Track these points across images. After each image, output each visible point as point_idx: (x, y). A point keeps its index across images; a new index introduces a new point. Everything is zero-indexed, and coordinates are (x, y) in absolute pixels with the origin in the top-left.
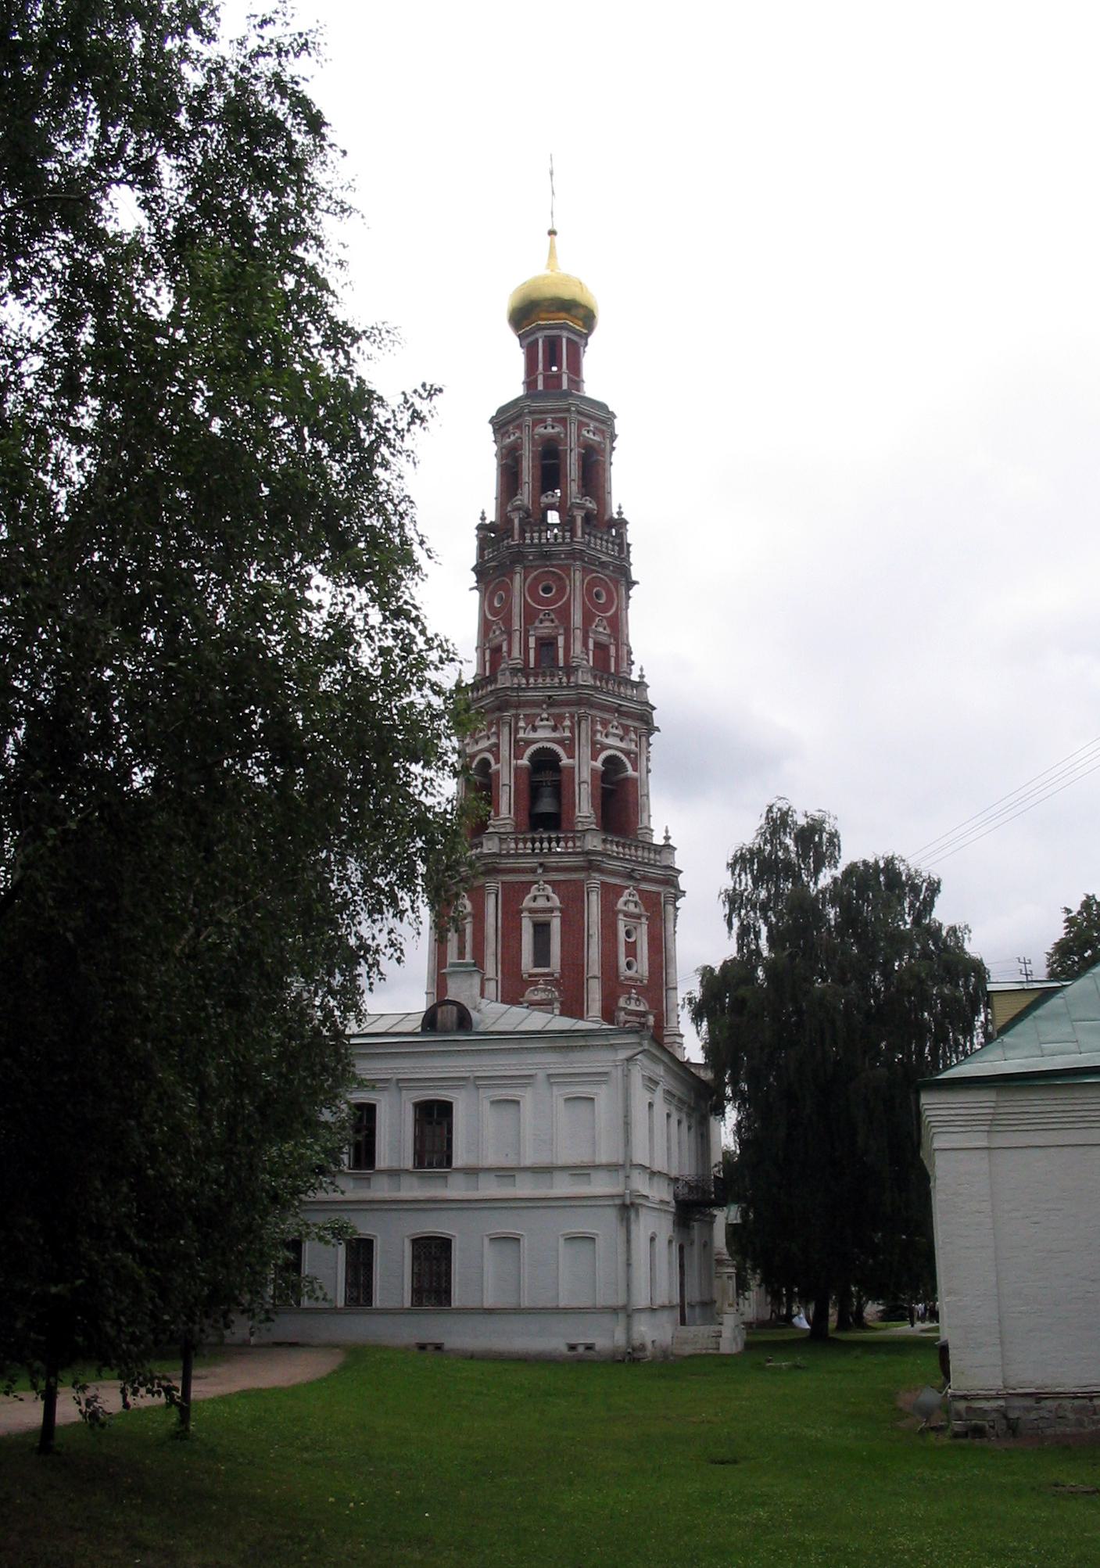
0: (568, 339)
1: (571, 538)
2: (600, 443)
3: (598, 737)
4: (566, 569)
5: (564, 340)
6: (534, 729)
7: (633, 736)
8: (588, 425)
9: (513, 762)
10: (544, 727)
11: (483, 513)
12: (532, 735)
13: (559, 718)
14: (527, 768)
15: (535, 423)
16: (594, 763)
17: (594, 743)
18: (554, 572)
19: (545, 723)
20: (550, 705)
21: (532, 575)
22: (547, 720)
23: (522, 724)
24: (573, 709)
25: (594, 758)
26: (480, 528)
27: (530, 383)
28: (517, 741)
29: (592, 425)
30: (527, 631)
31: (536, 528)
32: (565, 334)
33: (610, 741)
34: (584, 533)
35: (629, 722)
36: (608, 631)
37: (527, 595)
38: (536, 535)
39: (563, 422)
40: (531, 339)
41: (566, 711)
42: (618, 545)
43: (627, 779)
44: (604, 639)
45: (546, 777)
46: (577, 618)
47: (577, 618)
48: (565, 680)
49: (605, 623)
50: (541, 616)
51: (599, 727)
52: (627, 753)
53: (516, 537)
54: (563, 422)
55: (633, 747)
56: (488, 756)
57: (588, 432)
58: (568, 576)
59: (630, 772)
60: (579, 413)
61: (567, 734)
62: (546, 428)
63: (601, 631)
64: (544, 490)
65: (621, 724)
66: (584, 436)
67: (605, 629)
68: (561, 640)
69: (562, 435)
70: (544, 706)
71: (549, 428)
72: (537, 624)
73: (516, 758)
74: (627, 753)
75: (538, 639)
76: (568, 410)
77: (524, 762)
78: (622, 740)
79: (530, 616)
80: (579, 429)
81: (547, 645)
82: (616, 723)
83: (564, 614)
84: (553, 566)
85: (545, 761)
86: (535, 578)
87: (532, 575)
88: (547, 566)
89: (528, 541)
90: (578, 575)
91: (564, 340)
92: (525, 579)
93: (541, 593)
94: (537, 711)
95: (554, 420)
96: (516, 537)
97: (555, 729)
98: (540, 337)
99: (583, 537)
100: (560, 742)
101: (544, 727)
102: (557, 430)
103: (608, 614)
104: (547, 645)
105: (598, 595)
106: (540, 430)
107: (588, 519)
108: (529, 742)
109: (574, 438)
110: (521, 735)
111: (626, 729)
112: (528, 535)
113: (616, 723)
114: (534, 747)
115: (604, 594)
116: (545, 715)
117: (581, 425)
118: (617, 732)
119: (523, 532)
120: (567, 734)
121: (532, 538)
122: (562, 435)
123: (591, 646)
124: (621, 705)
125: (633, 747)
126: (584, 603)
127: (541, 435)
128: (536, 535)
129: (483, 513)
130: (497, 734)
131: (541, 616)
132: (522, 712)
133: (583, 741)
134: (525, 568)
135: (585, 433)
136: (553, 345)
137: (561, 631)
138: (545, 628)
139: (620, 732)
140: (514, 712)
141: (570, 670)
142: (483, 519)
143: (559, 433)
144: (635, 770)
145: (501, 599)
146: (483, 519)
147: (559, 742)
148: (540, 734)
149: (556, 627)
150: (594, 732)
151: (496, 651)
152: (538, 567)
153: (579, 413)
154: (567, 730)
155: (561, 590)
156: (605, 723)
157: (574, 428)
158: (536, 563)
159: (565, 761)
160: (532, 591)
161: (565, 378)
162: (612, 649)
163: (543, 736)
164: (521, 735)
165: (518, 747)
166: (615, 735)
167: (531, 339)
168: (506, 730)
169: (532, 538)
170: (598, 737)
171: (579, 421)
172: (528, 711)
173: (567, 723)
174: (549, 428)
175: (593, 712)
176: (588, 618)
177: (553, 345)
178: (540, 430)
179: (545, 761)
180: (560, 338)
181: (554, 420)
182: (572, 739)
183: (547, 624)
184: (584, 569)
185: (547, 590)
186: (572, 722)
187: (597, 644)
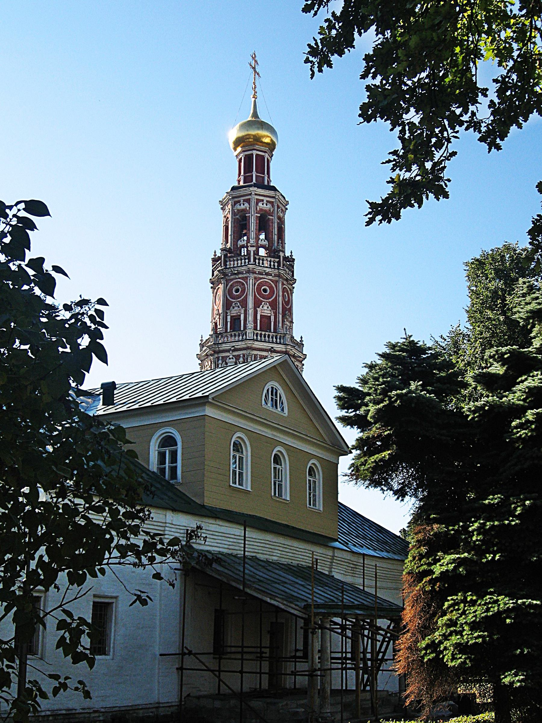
0: (257, 155)
1: (249, 262)
4: (245, 279)
10: (231, 362)
11: (215, 252)
15: (235, 203)
18: (240, 282)
19: (231, 360)
20: (233, 351)
21: (230, 284)
22: (233, 358)
29: (265, 199)
30: (227, 313)
31: (232, 259)
32: (255, 153)
39: (248, 201)
54: (248, 201)
57: (263, 204)
58: (247, 283)
60: (256, 194)
62: (240, 205)
63: (265, 310)
69: (248, 208)
75: (231, 317)
76: (250, 194)
84: (239, 278)
87: (230, 284)
88: (237, 279)
92: (227, 286)
93: (234, 293)
94: (228, 354)
95: (244, 201)
99: (255, 261)
105: (265, 290)
106: (238, 207)
112: (228, 263)
115: (268, 288)
116: (231, 357)
117: (258, 201)
121: (230, 264)
122: (248, 208)
124: (272, 348)
127: (238, 210)
128: (232, 263)
129: (215, 252)
136: (248, 159)
138: (234, 312)
142: (215, 255)
146: (215, 255)
153: (256, 194)
155: (243, 291)
158: (232, 277)
174: (242, 205)
175: (255, 352)
176: (257, 304)
178: (238, 207)
180: (252, 154)
184: (255, 278)
185: (237, 291)
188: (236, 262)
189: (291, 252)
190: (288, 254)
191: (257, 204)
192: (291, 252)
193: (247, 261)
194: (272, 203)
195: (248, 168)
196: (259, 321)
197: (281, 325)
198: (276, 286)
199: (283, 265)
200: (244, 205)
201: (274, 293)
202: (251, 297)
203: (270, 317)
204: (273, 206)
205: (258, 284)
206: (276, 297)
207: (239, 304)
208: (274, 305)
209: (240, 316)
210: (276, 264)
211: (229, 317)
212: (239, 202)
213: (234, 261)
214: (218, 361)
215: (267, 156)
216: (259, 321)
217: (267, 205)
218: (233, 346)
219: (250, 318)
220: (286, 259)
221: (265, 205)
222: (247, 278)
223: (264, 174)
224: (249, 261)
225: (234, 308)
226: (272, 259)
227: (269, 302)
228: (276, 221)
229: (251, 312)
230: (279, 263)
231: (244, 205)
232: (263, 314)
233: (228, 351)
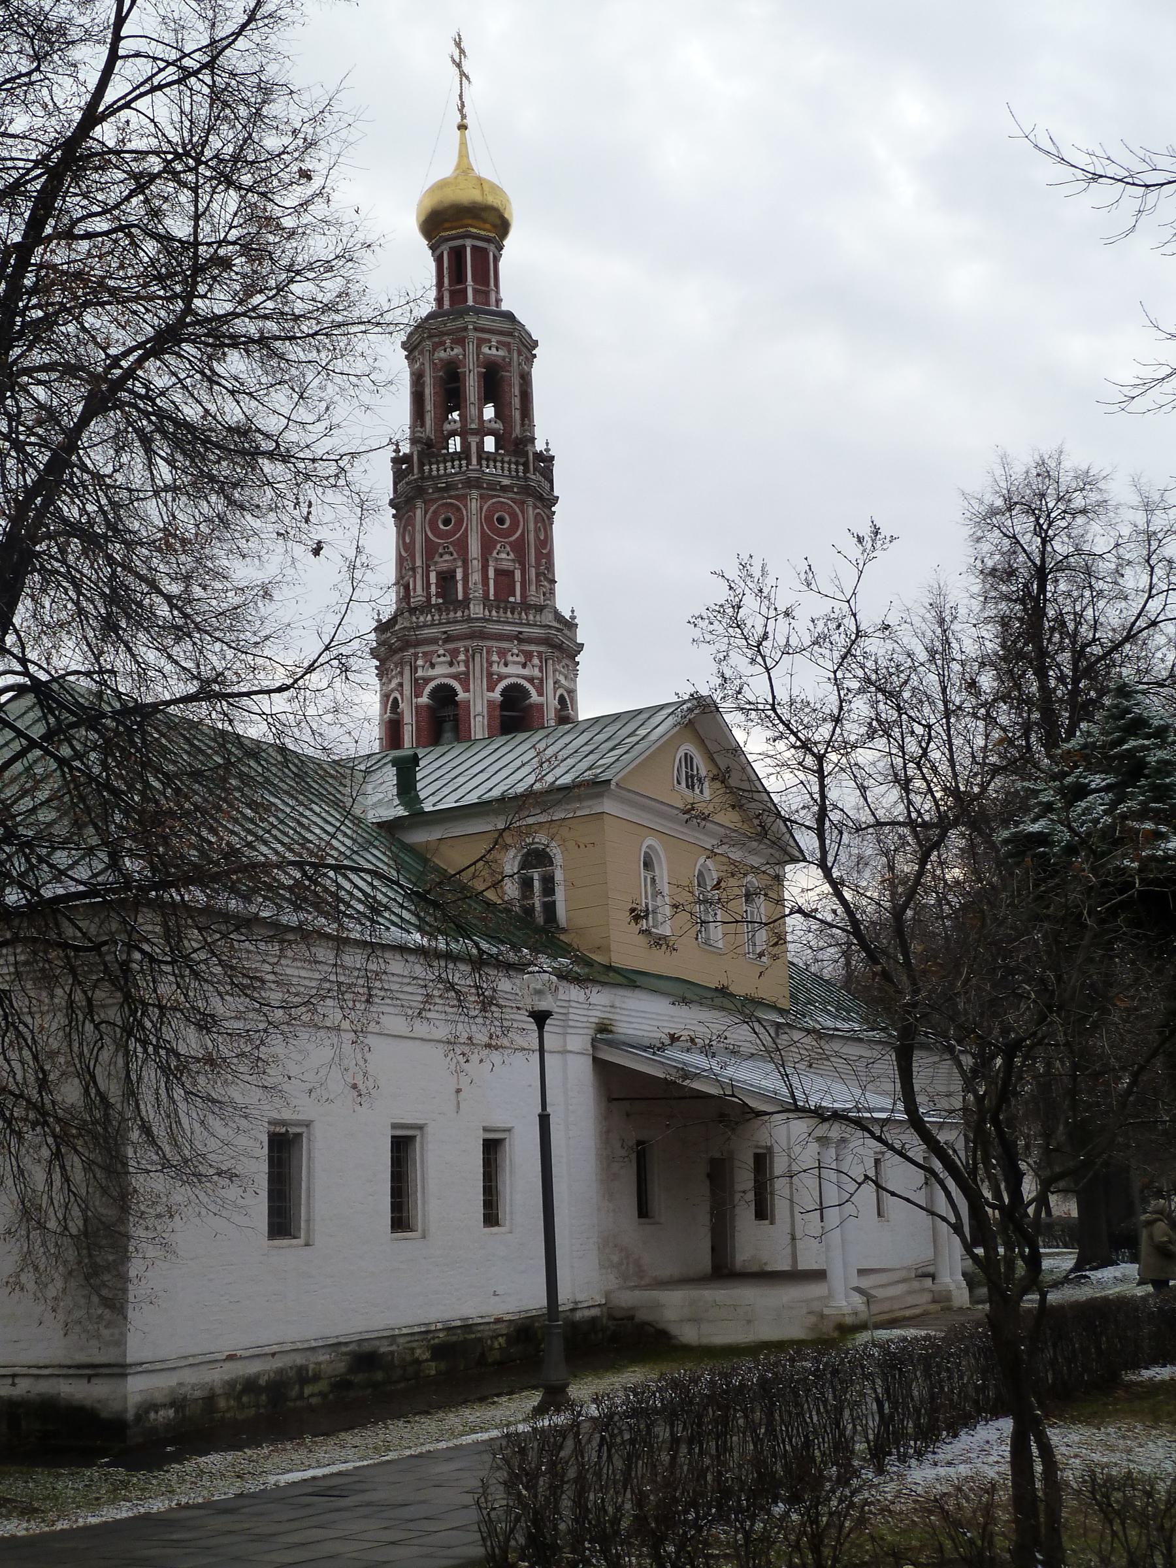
0: (474, 248)
2: (504, 358)
3: (495, 668)
4: (463, 498)
5: (468, 250)
6: (433, 666)
7: (536, 661)
8: (490, 341)
9: (414, 700)
10: (441, 663)
12: (431, 673)
13: (454, 653)
14: (428, 706)
15: (436, 346)
16: (491, 694)
17: (490, 675)
18: (451, 504)
19: (442, 659)
21: (432, 509)
23: (420, 662)
24: (467, 643)
25: (491, 689)
26: (394, 460)
27: (439, 300)
28: (416, 680)
29: (494, 339)
30: (428, 566)
31: (433, 460)
32: (469, 243)
33: (510, 670)
35: (532, 648)
36: (512, 556)
37: (427, 529)
38: (434, 467)
40: (438, 252)
41: (460, 645)
43: (531, 705)
44: (506, 566)
45: (448, 712)
46: (474, 548)
47: (474, 548)
48: (437, 617)
49: (508, 548)
51: (495, 658)
52: (531, 680)
54: (461, 342)
55: (536, 672)
56: (397, 694)
58: (465, 506)
59: (535, 697)
61: (462, 668)
63: (504, 558)
65: (520, 651)
66: (484, 354)
68: (459, 575)
70: (440, 643)
72: (437, 558)
73: (417, 697)
74: (531, 680)
75: (438, 574)
77: (424, 700)
78: (524, 666)
79: (431, 551)
80: (479, 347)
81: (446, 579)
82: (516, 651)
84: (450, 497)
85: (444, 696)
86: (434, 512)
87: (432, 509)
90: (474, 505)
91: (468, 250)
92: (426, 513)
93: (442, 527)
94: (434, 648)
97: (451, 664)
98: (445, 249)
99: (479, 463)
100: (455, 677)
101: (441, 663)
102: (456, 351)
104: (446, 579)
105: (501, 521)
106: (442, 354)
108: (427, 680)
110: (420, 673)
111: (529, 656)
112: (426, 468)
113: (516, 651)
114: (432, 684)
115: (507, 517)
116: (441, 652)
117: (480, 342)
120: (462, 668)
121: (431, 470)
123: (491, 574)
124: (521, 633)
125: (536, 672)
126: (483, 532)
127: (441, 360)
128: (434, 467)
130: (401, 673)
132: (420, 650)
133: (478, 674)
134: (425, 502)
135: (485, 350)
136: (458, 255)
137: (460, 563)
138: (443, 563)
140: (412, 651)
141: (465, 603)
143: (457, 355)
144: (540, 694)
147: (455, 677)
148: (439, 670)
149: (455, 559)
150: (490, 664)
151: (407, 587)
152: (436, 500)
153: (475, 329)
154: (462, 664)
155: (460, 521)
156: (502, 653)
159: (462, 695)
160: (433, 525)
163: (441, 673)
164: (420, 673)
165: (418, 685)
167: (438, 252)
168: (407, 669)
169: (438, 470)
170: (495, 668)
171: (479, 339)
172: (427, 649)
173: (462, 657)
175: (489, 643)
176: (487, 547)
177: (458, 255)
179: (444, 696)
180: (464, 247)
182: (467, 674)
183: (447, 557)
184: (482, 497)
185: (447, 522)
186: (466, 656)
187: (499, 572)
188: (442, 466)
189: (547, 444)
190: (540, 446)
191: (479, 347)
192: (547, 444)
194: (507, 345)
195: (458, 275)
196: (491, 582)
197: (533, 588)
198: (523, 513)
199: (535, 469)
201: (518, 526)
202: (474, 534)
203: (513, 572)
204: (509, 351)
205: (488, 510)
206: (523, 534)
207: (451, 549)
208: (519, 549)
210: (521, 468)
212: (443, 343)
214: (416, 661)
215: (492, 248)
216: (491, 582)
218: (445, 632)
219: (476, 577)
220: (539, 457)
221: (494, 351)
222: (464, 496)
223: (488, 285)
224: (468, 464)
226: (513, 460)
227: (510, 544)
228: (516, 381)
229: (476, 564)
230: (526, 464)
232: (499, 567)
233: (433, 641)
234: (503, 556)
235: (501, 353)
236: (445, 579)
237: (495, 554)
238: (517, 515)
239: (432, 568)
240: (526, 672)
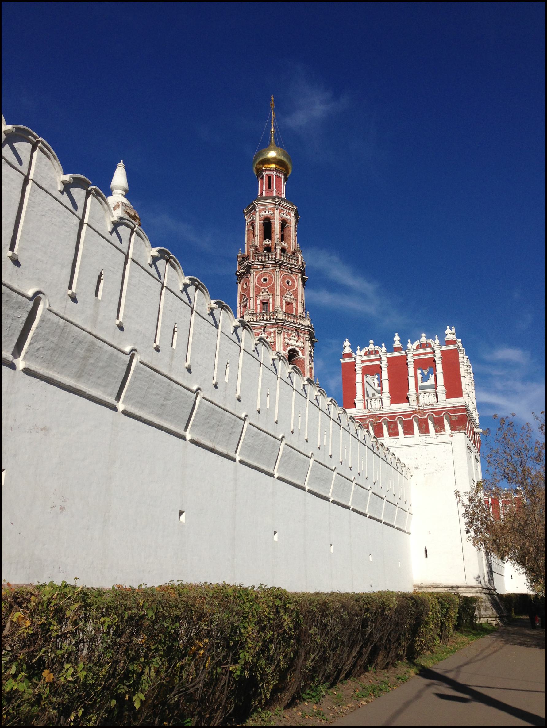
0: (276, 176)
7: (302, 340)
16: (284, 352)
21: (259, 274)
33: (292, 342)
34: (281, 255)
36: (293, 297)
39: (272, 209)
42: (297, 260)
50: (263, 291)
51: (286, 336)
53: (251, 259)
59: (301, 355)
61: (272, 339)
62: (265, 212)
64: (265, 239)
67: (291, 295)
68: (271, 301)
71: (267, 212)
72: (261, 294)
75: (261, 301)
81: (265, 303)
83: (272, 290)
87: (259, 274)
89: (257, 260)
95: (269, 209)
96: (251, 259)
102: (270, 213)
103: (294, 289)
104: (265, 303)
105: (288, 283)
106: (264, 213)
107: (283, 250)
109: (278, 216)
118: (295, 338)
119: (254, 256)
120: (272, 339)
126: (281, 285)
131: (263, 291)
134: (256, 272)
139: (296, 338)
143: (271, 214)
144: (303, 355)
145: (246, 284)
154: (272, 338)
156: (289, 335)
157: (278, 212)
161: (275, 192)
162: (294, 305)
166: (294, 340)
170: (286, 341)
173: (272, 335)
174: (267, 212)
181: (269, 209)
185: (265, 280)
187: (287, 303)
193: (274, 256)
200: (269, 212)
207: (267, 290)
209: (269, 300)
211: (258, 302)
213: (262, 256)
217: (286, 215)
221: (285, 215)
225: (263, 293)
231: (269, 212)
234: (288, 296)
235: (288, 217)
236: (264, 303)
237: (285, 295)
238: (294, 281)
239: (259, 297)
240: (299, 344)
